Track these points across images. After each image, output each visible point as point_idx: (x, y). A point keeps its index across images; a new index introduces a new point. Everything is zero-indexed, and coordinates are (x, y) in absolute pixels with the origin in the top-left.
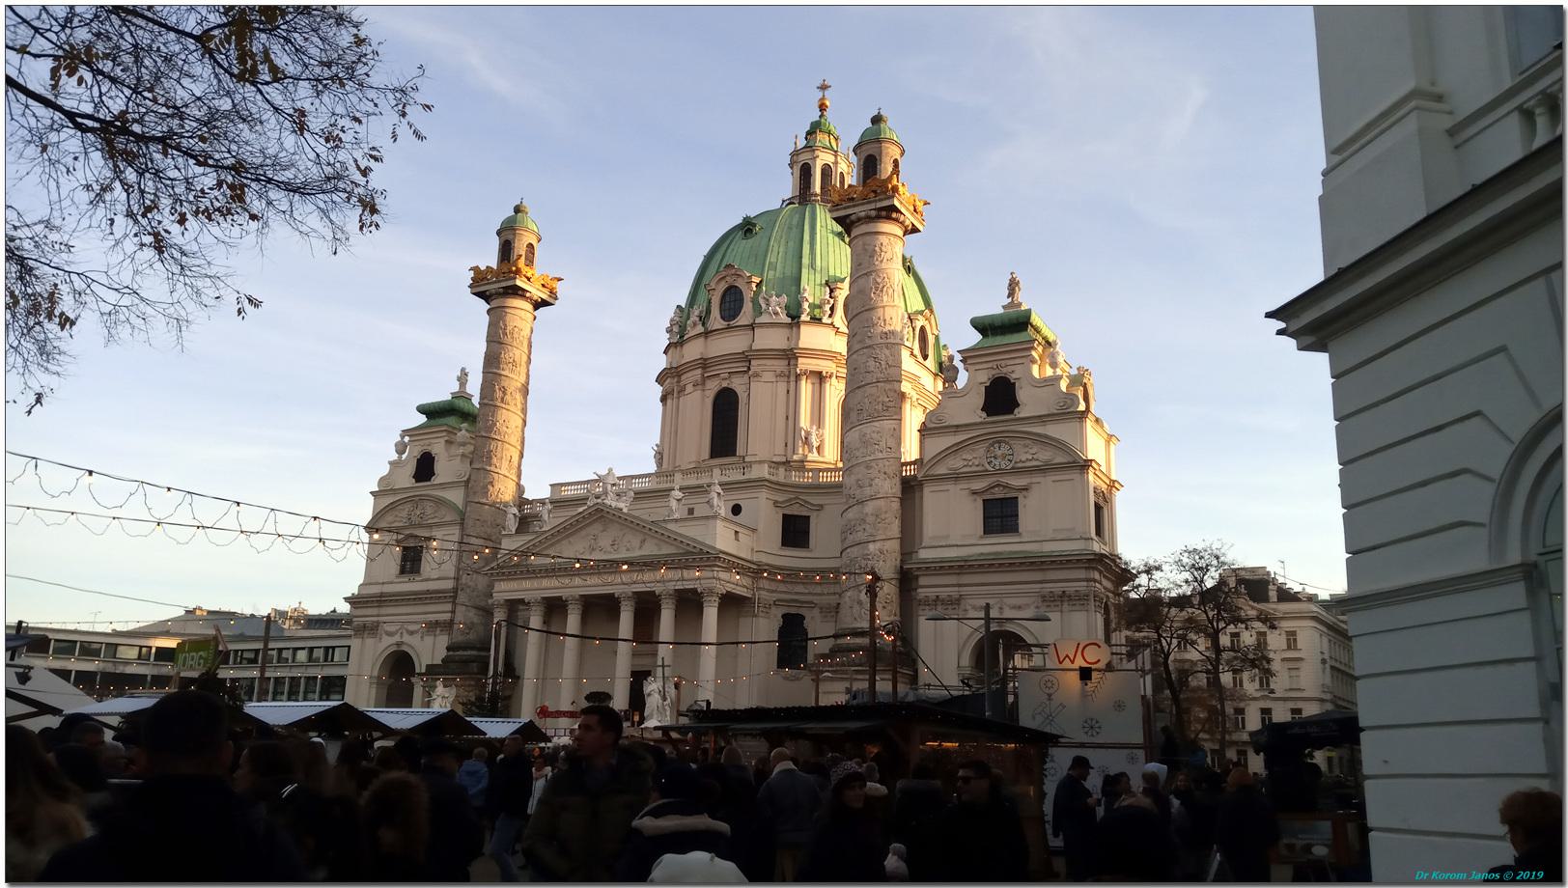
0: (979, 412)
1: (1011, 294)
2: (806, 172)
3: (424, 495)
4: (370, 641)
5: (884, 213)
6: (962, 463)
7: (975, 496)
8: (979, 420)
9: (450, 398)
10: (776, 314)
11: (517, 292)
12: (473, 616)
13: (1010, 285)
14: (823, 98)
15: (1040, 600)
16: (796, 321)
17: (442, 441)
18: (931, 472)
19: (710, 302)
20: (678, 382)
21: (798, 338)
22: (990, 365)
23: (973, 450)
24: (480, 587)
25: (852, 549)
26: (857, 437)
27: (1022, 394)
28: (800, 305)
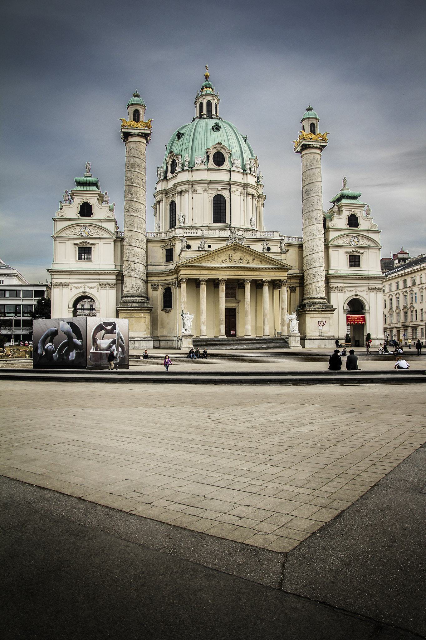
0: (347, 225)
2: (209, 104)
4: (65, 291)
5: (321, 147)
6: (343, 242)
7: (347, 254)
8: (347, 228)
11: (145, 136)
12: (140, 283)
15: (368, 289)
16: (245, 172)
17: (96, 198)
19: (208, 156)
21: (247, 179)
22: (350, 210)
24: (141, 270)
26: (316, 229)
27: (360, 221)
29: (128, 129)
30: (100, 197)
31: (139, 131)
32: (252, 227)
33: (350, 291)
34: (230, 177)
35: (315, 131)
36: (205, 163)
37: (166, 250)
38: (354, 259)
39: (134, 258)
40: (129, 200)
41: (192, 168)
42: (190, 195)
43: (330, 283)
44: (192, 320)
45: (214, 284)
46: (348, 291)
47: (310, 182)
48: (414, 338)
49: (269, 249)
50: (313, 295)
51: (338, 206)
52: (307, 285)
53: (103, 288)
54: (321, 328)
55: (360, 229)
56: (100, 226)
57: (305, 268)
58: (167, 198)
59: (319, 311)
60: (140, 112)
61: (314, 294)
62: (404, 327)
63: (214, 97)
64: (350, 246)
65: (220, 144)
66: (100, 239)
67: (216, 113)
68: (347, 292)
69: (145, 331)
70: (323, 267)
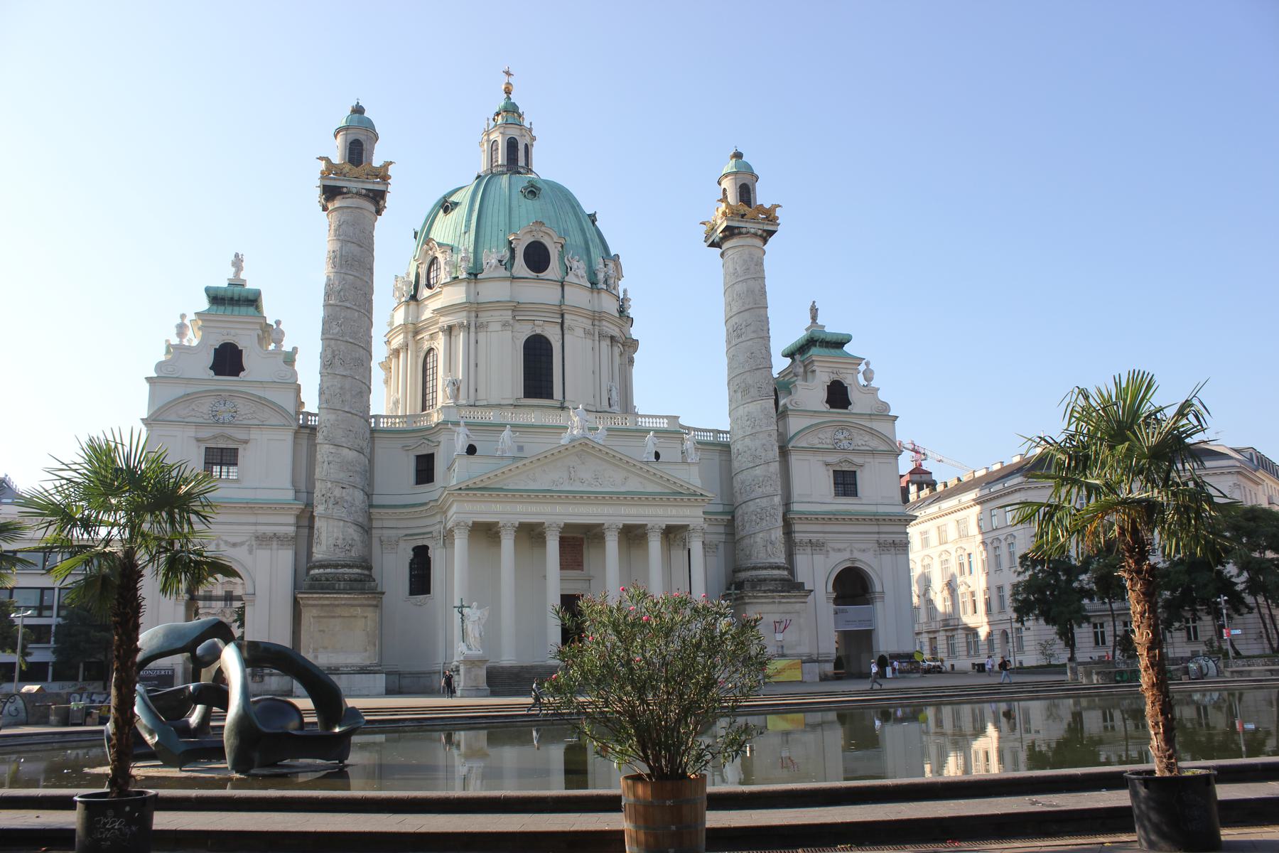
1: (814, 318)
3: (237, 391)
5: (765, 234)
9: (226, 285)
10: (582, 277)
12: (353, 533)
13: (811, 310)
14: (508, 83)
15: (877, 545)
18: (794, 445)
19: (512, 251)
20: (477, 317)
22: (830, 370)
23: (826, 432)
24: (357, 503)
25: (762, 500)
27: (853, 395)
28: (596, 275)
29: (334, 179)
30: (263, 332)
31: (360, 185)
32: (613, 408)
33: (839, 550)
34: (563, 297)
35: (750, 199)
36: (505, 263)
37: (418, 457)
38: (844, 478)
39: (342, 475)
40: (332, 339)
41: (476, 275)
42: (472, 335)
43: (794, 532)
44: (483, 621)
45: (531, 534)
46: (834, 550)
47: (743, 309)
48: (972, 653)
49: (657, 456)
50: (758, 561)
51: (803, 362)
52: (742, 538)
53: (264, 547)
54: (779, 637)
55: (853, 411)
56: (260, 398)
57: (740, 500)
58: (417, 342)
59: (774, 598)
60: (364, 146)
61: (760, 556)
62: (946, 630)
63: (524, 131)
64: (834, 450)
65: (542, 223)
66: (260, 426)
67: (527, 164)
68: (832, 554)
69: (366, 651)
70: (779, 497)
